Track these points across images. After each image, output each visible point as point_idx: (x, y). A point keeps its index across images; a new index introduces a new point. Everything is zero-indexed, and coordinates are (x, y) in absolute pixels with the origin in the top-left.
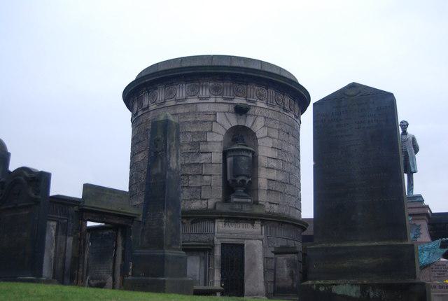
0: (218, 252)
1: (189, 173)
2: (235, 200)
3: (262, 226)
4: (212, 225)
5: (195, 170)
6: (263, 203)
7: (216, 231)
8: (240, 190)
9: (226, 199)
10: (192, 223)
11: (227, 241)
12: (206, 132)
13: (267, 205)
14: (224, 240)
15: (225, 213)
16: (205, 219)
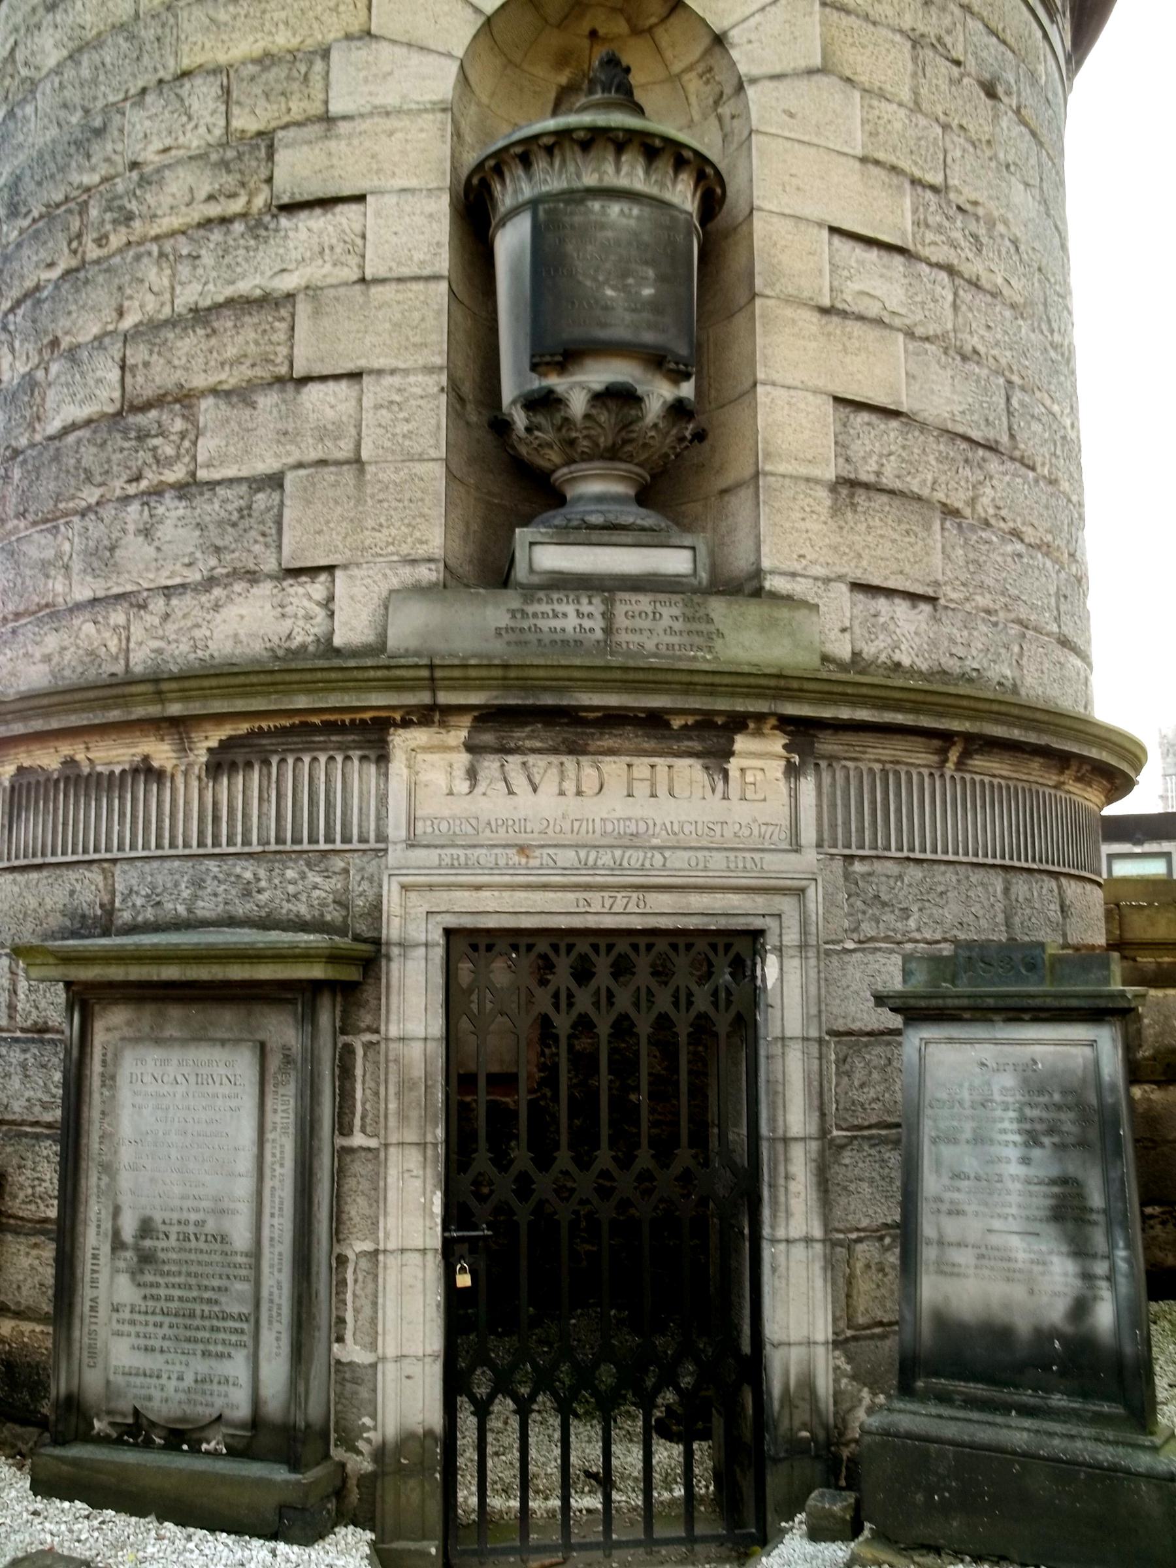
0: (413, 1009)
1: (199, 381)
2: (555, 558)
3: (792, 772)
4: (360, 776)
5: (241, 339)
6: (799, 588)
7: (396, 829)
8: (596, 487)
9: (490, 568)
10: (221, 763)
11: (498, 908)
12: (326, 54)
13: (839, 605)
14: (465, 900)
15: (464, 673)
16: (305, 733)
